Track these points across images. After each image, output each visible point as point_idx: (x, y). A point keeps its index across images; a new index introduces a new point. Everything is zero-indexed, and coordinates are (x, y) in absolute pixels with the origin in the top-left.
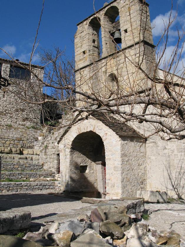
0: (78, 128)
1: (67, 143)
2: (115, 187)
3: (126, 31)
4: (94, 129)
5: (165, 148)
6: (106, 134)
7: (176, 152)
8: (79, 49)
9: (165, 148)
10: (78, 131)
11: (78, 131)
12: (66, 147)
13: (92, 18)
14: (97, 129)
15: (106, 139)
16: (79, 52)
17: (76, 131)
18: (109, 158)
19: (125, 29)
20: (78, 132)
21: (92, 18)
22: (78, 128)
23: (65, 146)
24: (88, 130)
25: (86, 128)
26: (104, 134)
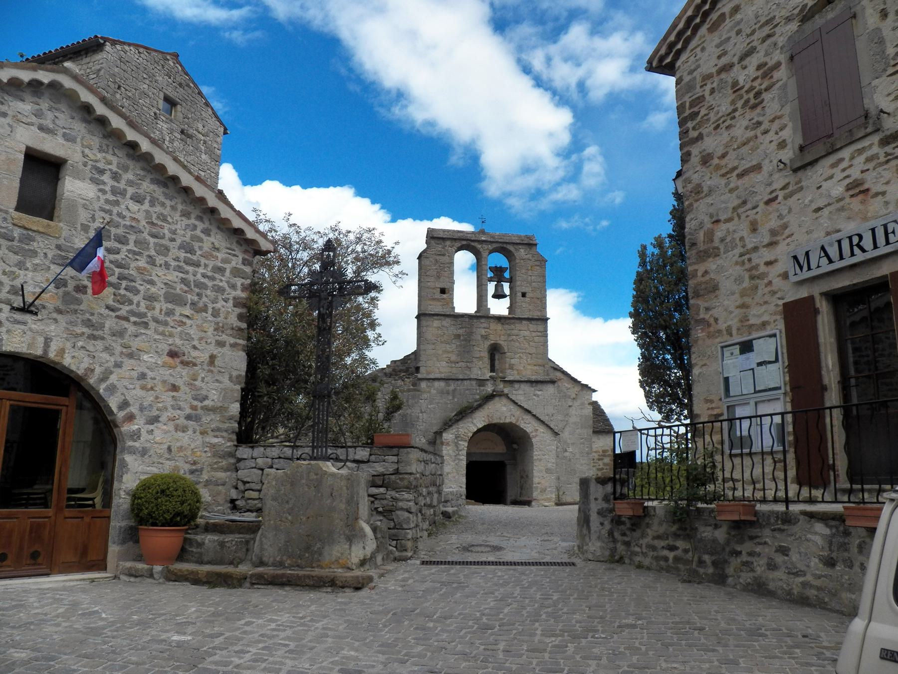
0: (488, 416)
3: (524, 295)
4: (518, 420)
5: (566, 451)
7: (577, 456)
8: (433, 279)
9: (566, 451)
15: (537, 436)
19: (524, 291)
20: (487, 421)
22: (488, 416)
23: (456, 438)
24: (508, 421)
25: (503, 418)
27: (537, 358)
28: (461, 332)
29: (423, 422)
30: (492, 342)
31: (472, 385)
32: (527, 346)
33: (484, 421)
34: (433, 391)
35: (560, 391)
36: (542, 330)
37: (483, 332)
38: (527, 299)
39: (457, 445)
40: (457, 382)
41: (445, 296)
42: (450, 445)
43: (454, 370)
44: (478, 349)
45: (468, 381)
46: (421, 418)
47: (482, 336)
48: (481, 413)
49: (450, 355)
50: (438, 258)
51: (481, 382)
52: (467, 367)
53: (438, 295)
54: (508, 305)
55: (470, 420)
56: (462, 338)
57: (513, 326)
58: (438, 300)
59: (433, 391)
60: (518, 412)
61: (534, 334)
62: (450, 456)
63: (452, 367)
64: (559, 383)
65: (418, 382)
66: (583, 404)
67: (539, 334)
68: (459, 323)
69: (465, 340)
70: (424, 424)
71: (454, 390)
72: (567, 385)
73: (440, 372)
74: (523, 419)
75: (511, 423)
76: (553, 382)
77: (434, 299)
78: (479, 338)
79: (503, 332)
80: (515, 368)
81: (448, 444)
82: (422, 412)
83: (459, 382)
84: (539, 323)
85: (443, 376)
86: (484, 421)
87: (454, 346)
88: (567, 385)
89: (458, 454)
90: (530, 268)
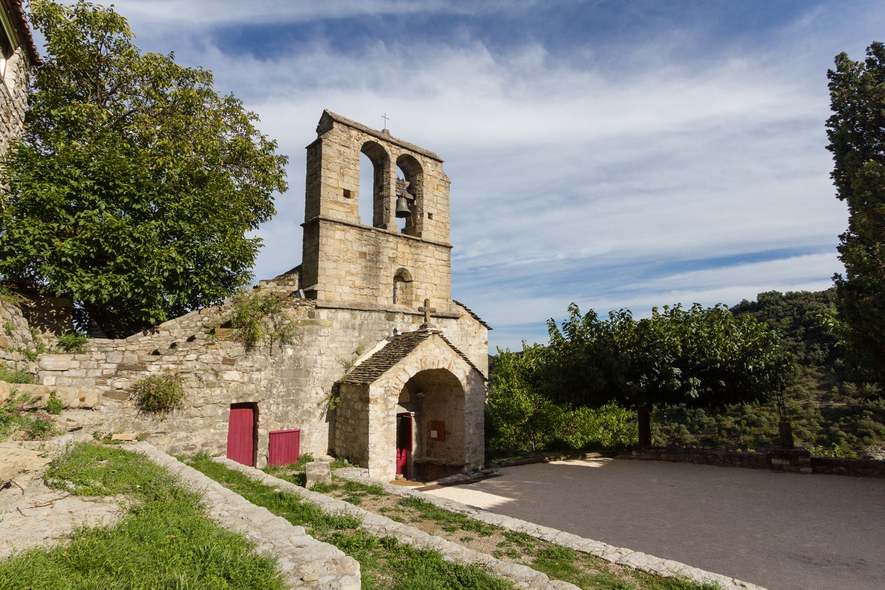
1: (394, 385)
3: (430, 216)
4: (449, 367)
13: (372, 139)
16: (334, 184)
17: (416, 365)
20: (420, 366)
21: (372, 139)
24: (440, 367)
25: (436, 362)
27: (442, 290)
28: (364, 249)
29: (322, 367)
30: (400, 267)
31: (380, 319)
32: (432, 275)
33: (417, 367)
34: (336, 325)
35: (462, 329)
36: (446, 259)
37: (391, 253)
38: (433, 222)
39: (386, 401)
40: (364, 314)
41: (349, 201)
42: (378, 403)
43: (359, 300)
44: (385, 273)
45: (377, 314)
46: (319, 362)
47: (389, 258)
48: (413, 357)
49: (354, 278)
50: (342, 149)
51: (390, 314)
52: (374, 295)
53: (341, 198)
54: (404, 226)
55: (402, 366)
56: (368, 257)
57: (419, 251)
58: (342, 204)
59: (336, 325)
60: (450, 354)
61: (439, 262)
62: (379, 420)
63: (356, 295)
64: (461, 320)
65: (316, 311)
66: (480, 343)
67: (444, 263)
68: (365, 238)
70: (323, 371)
71: (361, 325)
72: (468, 322)
74: (455, 363)
75: (443, 369)
76: (456, 318)
77: (336, 202)
78: (386, 259)
79: (410, 256)
81: (376, 401)
82: (321, 354)
83: (367, 314)
84: (444, 250)
85: (347, 305)
86: (417, 367)
87: (359, 267)
88: (468, 322)
89: (388, 415)
90: (436, 187)
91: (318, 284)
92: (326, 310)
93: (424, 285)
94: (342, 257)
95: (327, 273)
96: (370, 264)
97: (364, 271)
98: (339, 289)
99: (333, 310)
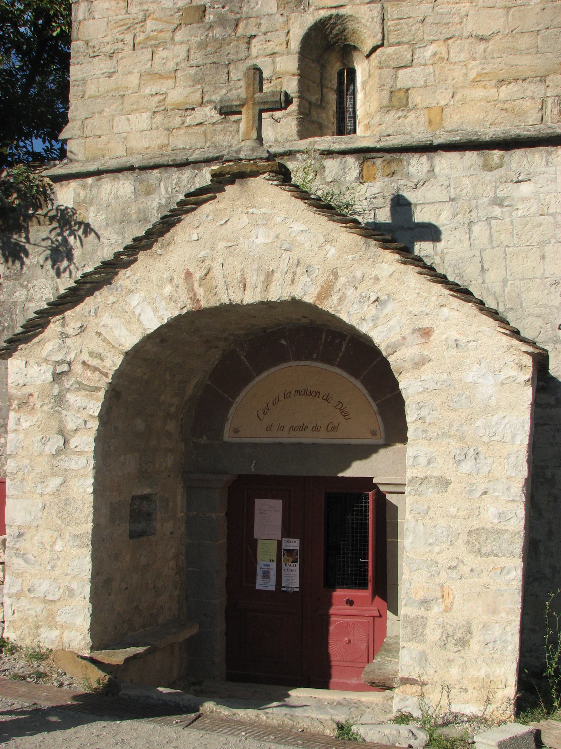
0: (189, 275)
1: (85, 357)
2: (475, 645)
6: (426, 333)
10: (191, 290)
11: (191, 290)
12: (68, 382)
14: (350, 292)
17: (168, 289)
18: (436, 474)
22: (189, 275)
23: (58, 377)
26: (407, 332)
27: (515, 51)
30: (323, 14)
44: (271, 47)
49: (164, 86)
56: (210, 17)
69: (222, 21)
73: (129, 152)
80: (416, 98)
81: (24, 403)
85: (135, 161)
91: (70, 125)
92: (74, 184)
93: (429, 51)
94: (129, 38)
95: (91, 90)
96: (218, 32)
97: (197, 57)
98: (121, 125)
99: (90, 180)
